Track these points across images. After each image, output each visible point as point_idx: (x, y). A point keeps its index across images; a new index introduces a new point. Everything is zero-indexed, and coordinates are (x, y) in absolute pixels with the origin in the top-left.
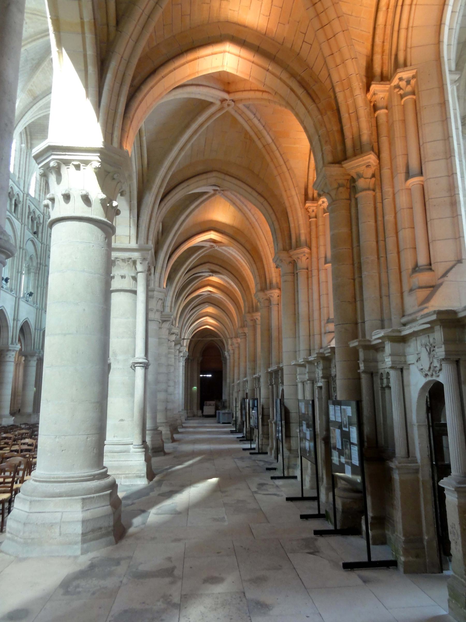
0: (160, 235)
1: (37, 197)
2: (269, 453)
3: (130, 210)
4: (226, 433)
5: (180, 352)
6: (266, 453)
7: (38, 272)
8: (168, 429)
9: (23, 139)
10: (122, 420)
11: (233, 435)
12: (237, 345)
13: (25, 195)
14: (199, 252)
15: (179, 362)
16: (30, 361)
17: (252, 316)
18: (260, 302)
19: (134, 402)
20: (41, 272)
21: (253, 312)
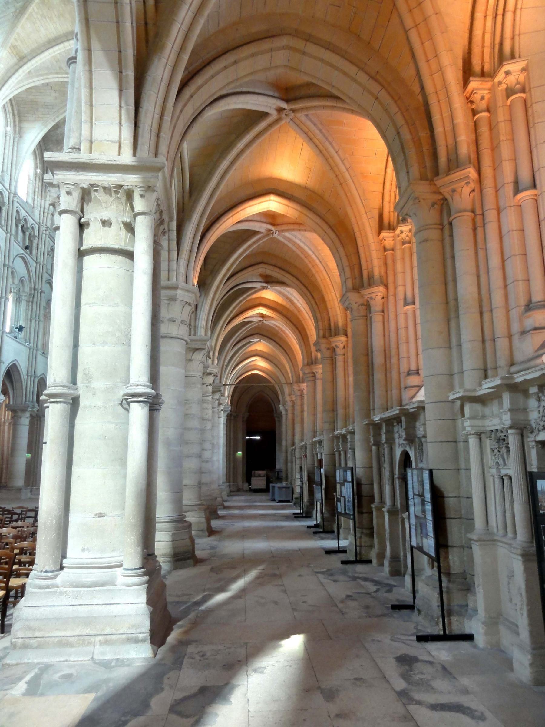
0: (187, 195)
1: (30, 201)
2: (374, 562)
3: (121, 91)
4: (287, 518)
5: (220, 404)
6: (369, 562)
7: (31, 299)
8: (203, 515)
9: (9, 120)
10: (100, 515)
11: (300, 521)
12: (298, 393)
13: (12, 195)
14: (249, 243)
15: (219, 417)
16: (20, 417)
17: (330, 343)
18: (352, 310)
19: (125, 476)
20: (35, 300)
21: (331, 336)
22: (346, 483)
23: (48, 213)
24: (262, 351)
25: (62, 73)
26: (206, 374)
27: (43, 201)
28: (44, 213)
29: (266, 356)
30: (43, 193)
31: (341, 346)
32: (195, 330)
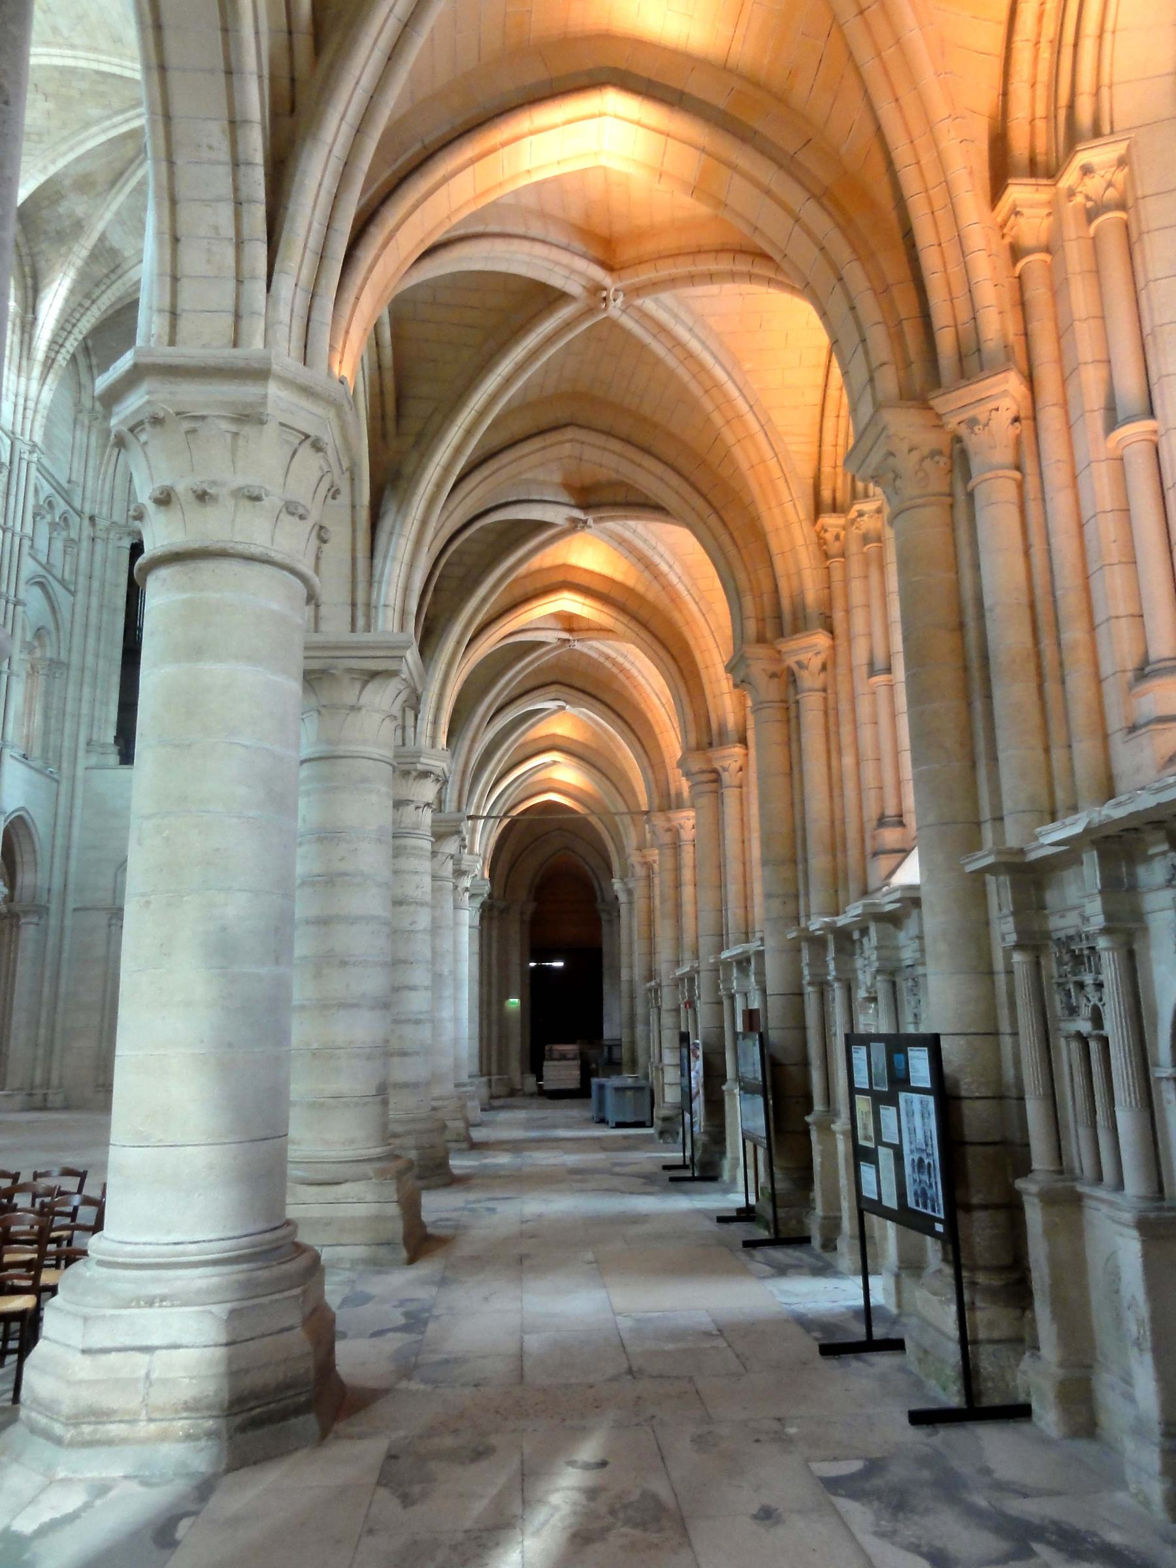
0: (303, 43)
4: (648, 1182)
5: (459, 873)
6: (1020, 1412)
8: (390, 1190)
11: (686, 1193)
12: (667, 838)
14: (531, 340)
15: (457, 907)
17: (779, 656)
18: (897, 476)
21: (780, 633)
22: (902, 1096)
23: (35, 411)
24: (568, 738)
25: (60, 46)
26: (414, 774)
27: (23, 380)
28: (25, 409)
29: (580, 750)
30: (24, 363)
31: (816, 663)
32: (368, 616)
